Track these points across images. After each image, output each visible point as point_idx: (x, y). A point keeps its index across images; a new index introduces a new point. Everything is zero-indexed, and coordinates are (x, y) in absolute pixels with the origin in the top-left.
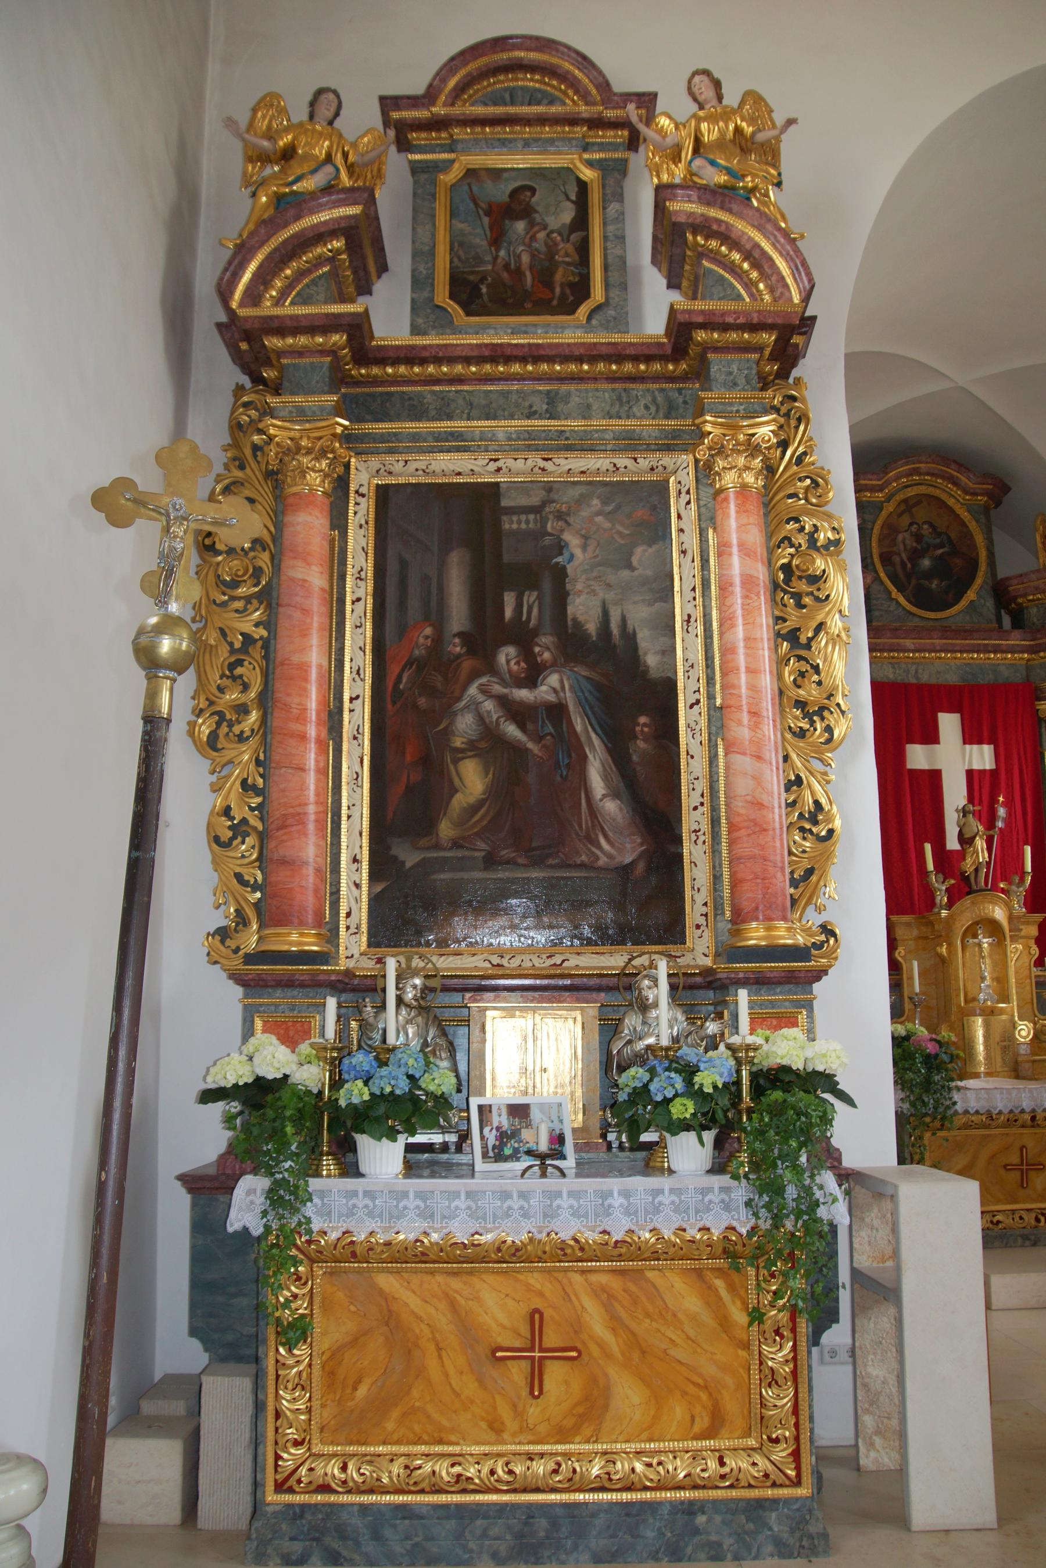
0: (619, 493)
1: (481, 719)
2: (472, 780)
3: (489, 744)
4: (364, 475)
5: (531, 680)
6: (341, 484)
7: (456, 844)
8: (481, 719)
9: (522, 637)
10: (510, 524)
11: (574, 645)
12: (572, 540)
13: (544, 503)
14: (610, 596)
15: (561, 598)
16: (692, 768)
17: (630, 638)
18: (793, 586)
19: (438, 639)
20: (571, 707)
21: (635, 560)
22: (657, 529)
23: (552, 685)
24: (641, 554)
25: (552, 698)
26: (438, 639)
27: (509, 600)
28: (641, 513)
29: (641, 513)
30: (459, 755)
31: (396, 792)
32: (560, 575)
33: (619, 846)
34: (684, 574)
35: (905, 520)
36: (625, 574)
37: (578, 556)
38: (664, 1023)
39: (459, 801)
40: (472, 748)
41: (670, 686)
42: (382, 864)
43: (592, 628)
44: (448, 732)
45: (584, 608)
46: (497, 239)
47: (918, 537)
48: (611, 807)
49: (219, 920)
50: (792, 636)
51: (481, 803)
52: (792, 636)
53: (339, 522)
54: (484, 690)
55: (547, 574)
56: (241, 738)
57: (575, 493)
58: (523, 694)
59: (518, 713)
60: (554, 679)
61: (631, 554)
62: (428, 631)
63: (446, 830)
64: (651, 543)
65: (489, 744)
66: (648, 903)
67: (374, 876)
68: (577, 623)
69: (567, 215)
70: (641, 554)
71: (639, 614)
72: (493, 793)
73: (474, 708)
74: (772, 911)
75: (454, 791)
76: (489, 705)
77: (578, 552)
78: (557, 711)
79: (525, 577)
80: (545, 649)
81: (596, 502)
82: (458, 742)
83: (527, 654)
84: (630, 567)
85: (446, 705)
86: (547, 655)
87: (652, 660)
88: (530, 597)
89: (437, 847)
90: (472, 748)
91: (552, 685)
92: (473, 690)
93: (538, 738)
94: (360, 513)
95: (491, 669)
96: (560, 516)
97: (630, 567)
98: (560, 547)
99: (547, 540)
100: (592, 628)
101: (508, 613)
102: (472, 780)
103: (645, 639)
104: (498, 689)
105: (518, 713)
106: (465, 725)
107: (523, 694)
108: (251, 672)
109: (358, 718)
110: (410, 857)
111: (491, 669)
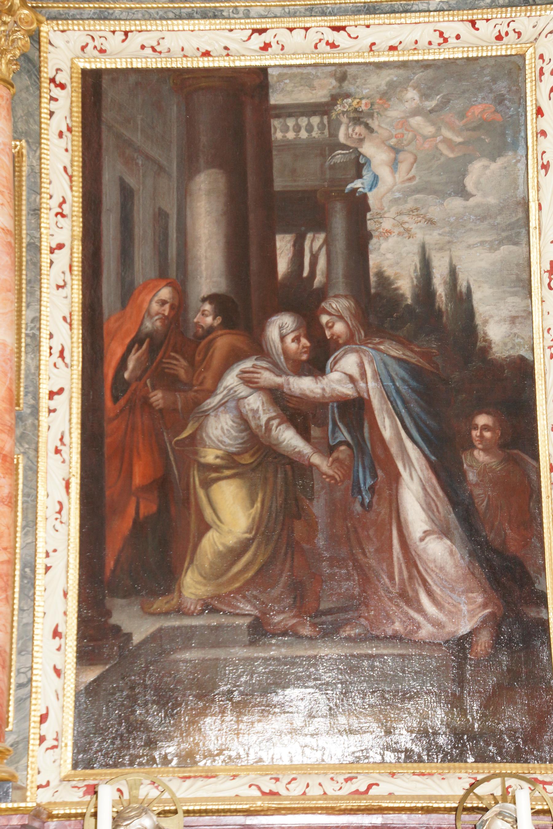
0: (448, 77)
1: (243, 421)
2: (232, 512)
3: (257, 458)
5: (317, 362)
7: (209, 607)
8: (243, 421)
9: (304, 301)
10: (283, 132)
11: (381, 312)
12: (375, 153)
13: (335, 99)
14: (433, 237)
15: (359, 241)
17: (463, 301)
19: (180, 307)
20: (376, 402)
21: (470, 183)
23: (348, 373)
24: (481, 174)
25: (347, 390)
26: (180, 307)
27: (284, 245)
28: (481, 108)
29: (481, 108)
30: (211, 474)
31: (120, 528)
32: (358, 207)
36: (456, 204)
37: (385, 182)
39: (212, 543)
42: (96, 637)
43: (405, 286)
44: (194, 440)
45: (393, 257)
51: (243, 547)
54: (248, 380)
55: (338, 206)
57: (379, 81)
58: (305, 385)
59: (300, 414)
60: (349, 363)
61: (464, 174)
62: (165, 293)
63: (193, 585)
64: (494, 155)
67: (85, 657)
68: (384, 281)
70: (481, 174)
71: (475, 264)
72: (262, 529)
73: (234, 405)
75: (205, 527)
76: (255, 402)
77: (384, 173)
78: (355, 410)
79: (307, 211)
81: (412, 94)
82: (210, 456)
84: (464, 193)
86: (339, 328)
87: (496, 332)
88: (314, 242)
89: (180, 611)
90: (231, 464)
91: (348, 373)
92: (231, 379)
93: (329, 450)
95: (258, 348)
96: (358, 118)
97: (464, 193)
98: (358, 166)
99: (339, 156)
100: (405, 286)
101: (283, 265)
102: (232, 512)
104: (268, 378)
105: (300, 414)
106: (220, 432)
107: (305, 385)
110: (137, 625)
111: (258, 348)
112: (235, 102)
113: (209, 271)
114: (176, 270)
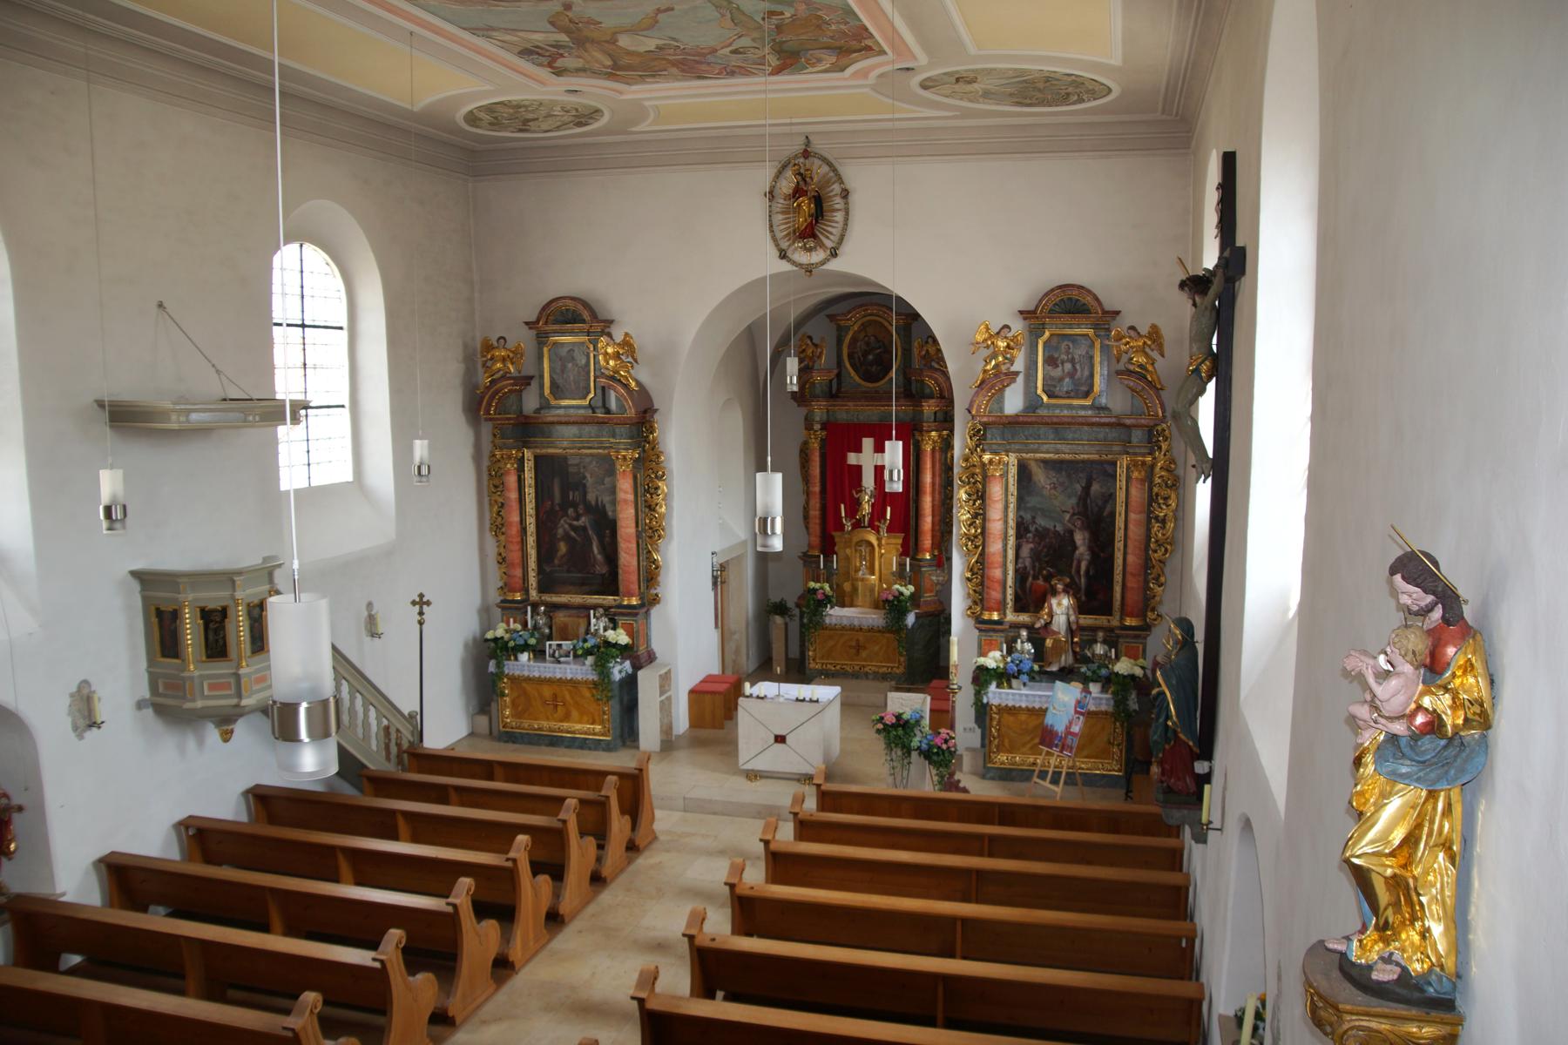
2: (563, 548)
3: (567, 537)
4: (528, 454)
5: (577, 519)
6: (521, 461)
9: (574, 505)
15: (585, 494)
22: (611, 472)
23: (583, 521)
24: (607, 480)
32: (584, 486)
33: (602, 569)
35: (862, 335)
37: (590, 480)
40: (563, 539)
45: (591, 497)
47: (868, 344)
48: (599, 557)
49: (501, 584)
50: (649, 507)
52: (649, 507)
53: (521, 470)
55: (581, 486)
65: (567, 537)
66: (610, 584)
70: (607, 480)
71: (606, 499)
73: (563, 526)
74: (630, 595)
78: (584, 528)
80: (581, 509)
90: (563, 539)
91: (583, 521)
94: (529, 466)
102: (563, 548)
103: (609, 508)
106: (560, 531)
109: (531, 528)
110: (548, 569)
114: (552, 498)
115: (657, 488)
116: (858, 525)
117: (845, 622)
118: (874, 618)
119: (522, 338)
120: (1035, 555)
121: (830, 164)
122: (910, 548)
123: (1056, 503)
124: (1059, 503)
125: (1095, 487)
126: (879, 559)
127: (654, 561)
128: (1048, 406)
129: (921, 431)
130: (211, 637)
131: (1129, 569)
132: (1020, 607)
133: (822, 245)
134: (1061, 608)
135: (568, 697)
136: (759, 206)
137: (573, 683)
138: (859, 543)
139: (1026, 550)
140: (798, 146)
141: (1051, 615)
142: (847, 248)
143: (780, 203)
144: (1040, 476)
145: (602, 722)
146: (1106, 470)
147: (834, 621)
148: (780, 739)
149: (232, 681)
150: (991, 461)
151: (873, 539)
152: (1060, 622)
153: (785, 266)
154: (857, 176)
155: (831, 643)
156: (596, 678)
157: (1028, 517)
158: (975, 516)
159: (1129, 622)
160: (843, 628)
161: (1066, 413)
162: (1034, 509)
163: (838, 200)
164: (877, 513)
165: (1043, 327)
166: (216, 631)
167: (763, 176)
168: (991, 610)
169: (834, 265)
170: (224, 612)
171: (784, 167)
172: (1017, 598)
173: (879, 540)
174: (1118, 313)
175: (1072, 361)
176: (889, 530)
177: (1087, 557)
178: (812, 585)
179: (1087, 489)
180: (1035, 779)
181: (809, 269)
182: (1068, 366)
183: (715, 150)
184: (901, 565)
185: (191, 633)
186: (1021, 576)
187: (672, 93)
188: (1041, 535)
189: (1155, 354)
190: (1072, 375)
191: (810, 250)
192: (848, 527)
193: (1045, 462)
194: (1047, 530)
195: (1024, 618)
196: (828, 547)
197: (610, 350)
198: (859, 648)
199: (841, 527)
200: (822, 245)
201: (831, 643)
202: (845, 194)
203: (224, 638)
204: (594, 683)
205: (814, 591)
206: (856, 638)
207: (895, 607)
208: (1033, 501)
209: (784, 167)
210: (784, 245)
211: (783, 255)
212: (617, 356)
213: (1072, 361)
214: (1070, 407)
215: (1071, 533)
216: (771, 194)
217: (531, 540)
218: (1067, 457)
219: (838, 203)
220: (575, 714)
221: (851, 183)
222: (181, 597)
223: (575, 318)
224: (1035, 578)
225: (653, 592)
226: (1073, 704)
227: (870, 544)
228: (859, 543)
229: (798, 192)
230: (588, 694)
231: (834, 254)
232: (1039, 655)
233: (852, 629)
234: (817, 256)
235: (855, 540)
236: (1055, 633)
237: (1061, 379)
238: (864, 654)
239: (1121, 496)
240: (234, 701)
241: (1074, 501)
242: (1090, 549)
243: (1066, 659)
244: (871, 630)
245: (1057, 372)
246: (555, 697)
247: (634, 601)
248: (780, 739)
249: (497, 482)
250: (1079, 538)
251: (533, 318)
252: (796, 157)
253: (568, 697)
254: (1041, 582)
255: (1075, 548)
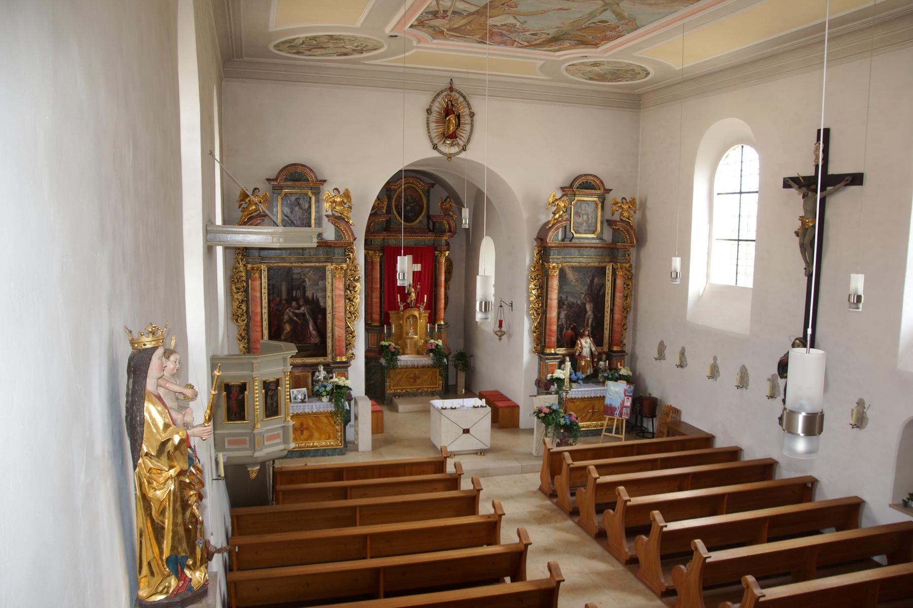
2: (288, 328)
3: (291, 321)
5: (299, 309)
11: (307, 301)
12: (307, 280)
15: (305, 292)
16: (329, 325)
17: (318, 300)
18: (349, 287)
19: (281, 300)
22: (323, 277)
24: (320, 283)
26: (281, 300)
31: (274, 329)
32: (304, 287)
33: (315, 340)
34: (329, 287)
37: (308, 283)
38: (322, 374)
39: (285, 332)
41: (325, 310)
45: (309, 294)
46: (292, 211)
50: (349, 299)
52: (349, 299)
56: (243, 321)
65: (291, 321)
66: (320, 350)
69: (307, 206)
70: (320, 283)
71: (320, 295)
73: (288, 313)
74: (341, 355)
78: (304, 314)
80: (301, 302)
83: (298, 304)
85: (282, 313)
95: (291, 306)
98: (304, 281)
102: (288, 328)
103: (320, 300)
106: (286, 317)
108: (244, 307)
109: (265, 316)
111: (291, 306)
112: (289, 270)
113: (284, 296)
115: (354, 287)
116: (407, 307)
117: (409, 364)
118: (426, 360)
119: (265, 189)
120: (567, 317)
121: (464, 97)
122: (432, 319)
123: (578, 289)
124: (579, 289)
125: (596, 280)
126: (416, 326)
127: (352, 333)
128: (578, 238)
129: (441, 252)
130: (269, 401)
131: (615, 322)
132: (560, 345)
133: (458, 144)
134: (586, 344)
135: (311, 423)
136: (422, 116)
137: (316, 416)
138: (408, 318)
139: (562, 316)
140: (445, 84)
141: (582, 348)
142: (470, 147)
143: (434, 116)
144: (570, 275)
145: (335, 438)
146: (602, 271)
147: (403, 364)
148: (466, 431)
149: (281, 432)
150: (253, 269)
151: (416, 313)
152: (586, 352)
153: (435, 154)
154: (481, 106)
155: (399, 377)
156: (333, 410)
157: (564, 297)
158: (538, 297)
159: (615, 348)
160: (407, 367)
161: (586, 241)
162: (567, 292)
163: (468, 118)
164: (419, 299)
165: (575, 195)
166: (272, 396)
167: (424, 100)
168: (550, 348)
169: (463, 155)
170: (277, 382)
171: (438, 95)
172: (558, 340)
173: (420, 314)
174: (611, 190)
175: (587, 214)
176: (425, 309)
177: (592, 316)
178: (383, 343)
179: (592, 281)
180: (604, 433)
181: (450, 157)
182: (585, 217)
183: (400, 81)
184: (432, 329)
185: (256, 399)
186: (560, 328)
187: (445, 47)
188: (571, 306)
189: (632, 212)
190: (587, 222)
191: (452, 145)
192: (402, 307)
193: (573, 267)
194: (573, 303)
195: (562, 351)
196: (385, 320)
197: (338, 200)
198: (416, 378)
199: (396, 308)
200: (458, 144)
201: (399, 377)
202: (472, 115)
203: (277, 402)
204: (332, 414)
205: (387, 347)
206: (414, 372)
207: (436, 351)
208: (566, 288)
209: (438, 95)
210: (436, 141)
211: (435, 147)
212: (342, 203)
213: (587, 214)
214: (587, 238)
215: (584, 304)
216: (429, 111)
217: (265, 324)
218: (583, 265)
219: (466, 119)
220: (316, 434)
221: (474, 110)
222: (255, 374)
223: (592, 187)
224: (567, 329)
225: (350, 352)
226: (622, 391)
227: (415, 317)
228: (408, 318)
229: (448, 111)
230: (325, 420)
231: (464, 149)
232: (575, 367)
233: (413, 367)
234: (454, 150)
235: (407, 315)
236: (585, 357)
237: (582, 224)
238: (418, 381)
239: (609, 285)
240: (282, 447)
241: (586, 287)
242: (593, 312)
243: (589, 371)
244: (423, 367)
245: (580, 220)
246: (302, 424)
247: (344, 359)
248: (466, 431)
249: (238, 285)
250: (589, 307)
251: (273, 175)
252: (446, 90)
253: (311, 423)
254: (570, 331)
255: (586, 312)
